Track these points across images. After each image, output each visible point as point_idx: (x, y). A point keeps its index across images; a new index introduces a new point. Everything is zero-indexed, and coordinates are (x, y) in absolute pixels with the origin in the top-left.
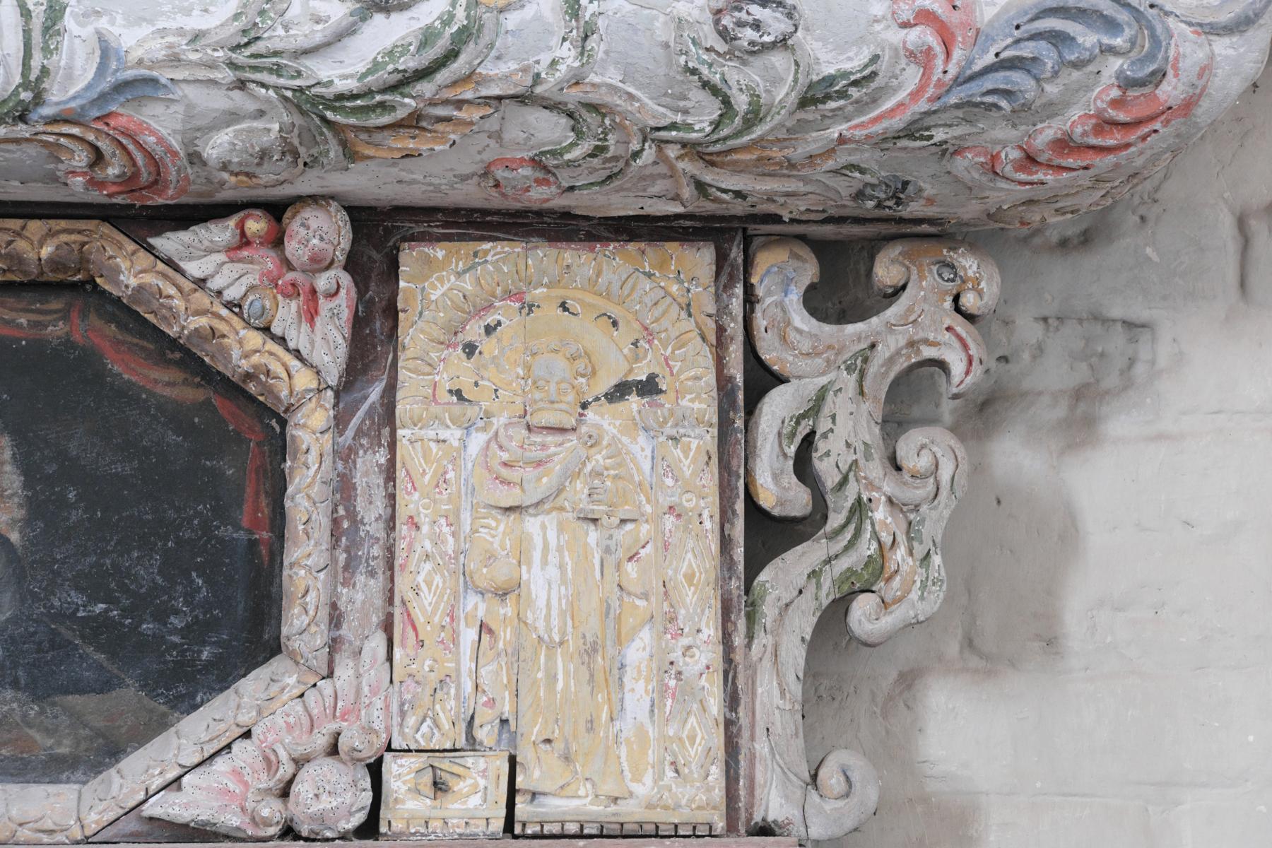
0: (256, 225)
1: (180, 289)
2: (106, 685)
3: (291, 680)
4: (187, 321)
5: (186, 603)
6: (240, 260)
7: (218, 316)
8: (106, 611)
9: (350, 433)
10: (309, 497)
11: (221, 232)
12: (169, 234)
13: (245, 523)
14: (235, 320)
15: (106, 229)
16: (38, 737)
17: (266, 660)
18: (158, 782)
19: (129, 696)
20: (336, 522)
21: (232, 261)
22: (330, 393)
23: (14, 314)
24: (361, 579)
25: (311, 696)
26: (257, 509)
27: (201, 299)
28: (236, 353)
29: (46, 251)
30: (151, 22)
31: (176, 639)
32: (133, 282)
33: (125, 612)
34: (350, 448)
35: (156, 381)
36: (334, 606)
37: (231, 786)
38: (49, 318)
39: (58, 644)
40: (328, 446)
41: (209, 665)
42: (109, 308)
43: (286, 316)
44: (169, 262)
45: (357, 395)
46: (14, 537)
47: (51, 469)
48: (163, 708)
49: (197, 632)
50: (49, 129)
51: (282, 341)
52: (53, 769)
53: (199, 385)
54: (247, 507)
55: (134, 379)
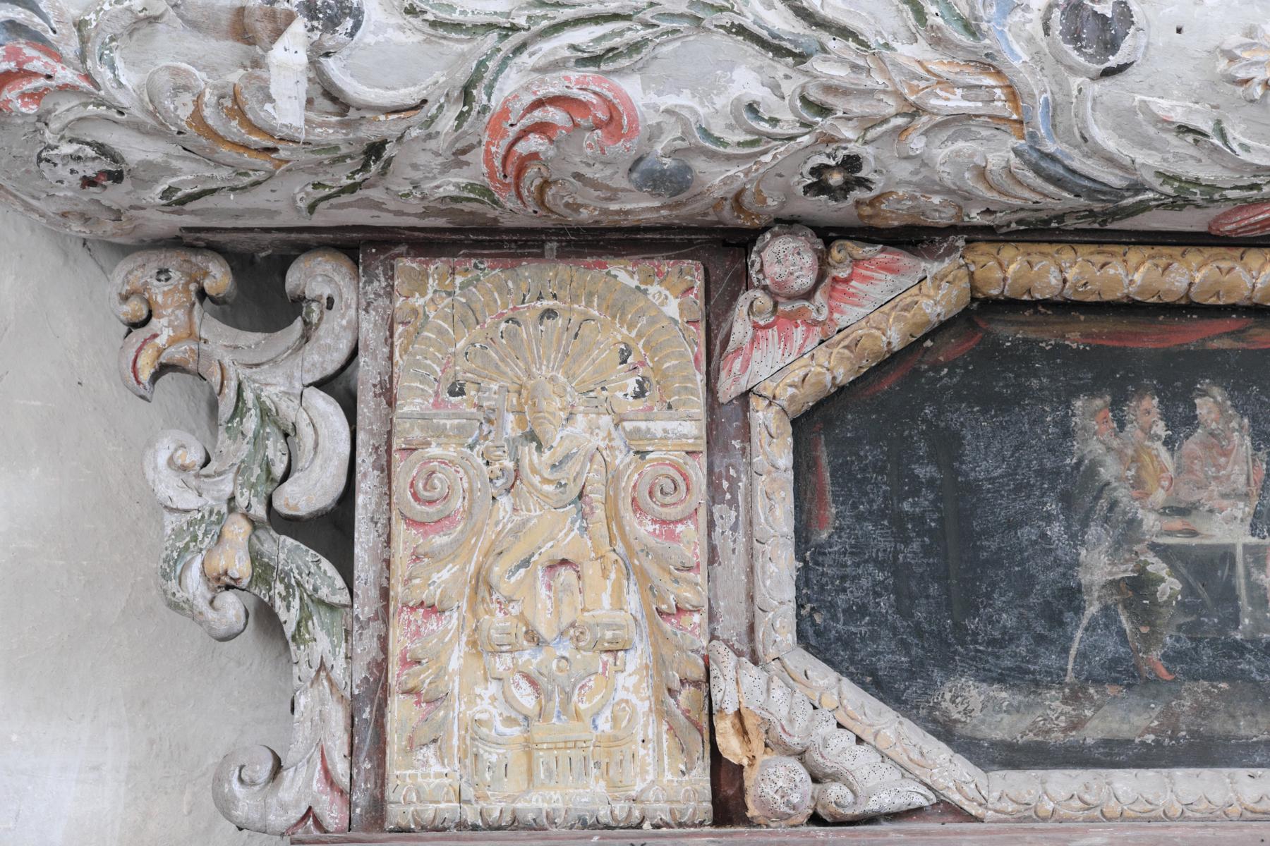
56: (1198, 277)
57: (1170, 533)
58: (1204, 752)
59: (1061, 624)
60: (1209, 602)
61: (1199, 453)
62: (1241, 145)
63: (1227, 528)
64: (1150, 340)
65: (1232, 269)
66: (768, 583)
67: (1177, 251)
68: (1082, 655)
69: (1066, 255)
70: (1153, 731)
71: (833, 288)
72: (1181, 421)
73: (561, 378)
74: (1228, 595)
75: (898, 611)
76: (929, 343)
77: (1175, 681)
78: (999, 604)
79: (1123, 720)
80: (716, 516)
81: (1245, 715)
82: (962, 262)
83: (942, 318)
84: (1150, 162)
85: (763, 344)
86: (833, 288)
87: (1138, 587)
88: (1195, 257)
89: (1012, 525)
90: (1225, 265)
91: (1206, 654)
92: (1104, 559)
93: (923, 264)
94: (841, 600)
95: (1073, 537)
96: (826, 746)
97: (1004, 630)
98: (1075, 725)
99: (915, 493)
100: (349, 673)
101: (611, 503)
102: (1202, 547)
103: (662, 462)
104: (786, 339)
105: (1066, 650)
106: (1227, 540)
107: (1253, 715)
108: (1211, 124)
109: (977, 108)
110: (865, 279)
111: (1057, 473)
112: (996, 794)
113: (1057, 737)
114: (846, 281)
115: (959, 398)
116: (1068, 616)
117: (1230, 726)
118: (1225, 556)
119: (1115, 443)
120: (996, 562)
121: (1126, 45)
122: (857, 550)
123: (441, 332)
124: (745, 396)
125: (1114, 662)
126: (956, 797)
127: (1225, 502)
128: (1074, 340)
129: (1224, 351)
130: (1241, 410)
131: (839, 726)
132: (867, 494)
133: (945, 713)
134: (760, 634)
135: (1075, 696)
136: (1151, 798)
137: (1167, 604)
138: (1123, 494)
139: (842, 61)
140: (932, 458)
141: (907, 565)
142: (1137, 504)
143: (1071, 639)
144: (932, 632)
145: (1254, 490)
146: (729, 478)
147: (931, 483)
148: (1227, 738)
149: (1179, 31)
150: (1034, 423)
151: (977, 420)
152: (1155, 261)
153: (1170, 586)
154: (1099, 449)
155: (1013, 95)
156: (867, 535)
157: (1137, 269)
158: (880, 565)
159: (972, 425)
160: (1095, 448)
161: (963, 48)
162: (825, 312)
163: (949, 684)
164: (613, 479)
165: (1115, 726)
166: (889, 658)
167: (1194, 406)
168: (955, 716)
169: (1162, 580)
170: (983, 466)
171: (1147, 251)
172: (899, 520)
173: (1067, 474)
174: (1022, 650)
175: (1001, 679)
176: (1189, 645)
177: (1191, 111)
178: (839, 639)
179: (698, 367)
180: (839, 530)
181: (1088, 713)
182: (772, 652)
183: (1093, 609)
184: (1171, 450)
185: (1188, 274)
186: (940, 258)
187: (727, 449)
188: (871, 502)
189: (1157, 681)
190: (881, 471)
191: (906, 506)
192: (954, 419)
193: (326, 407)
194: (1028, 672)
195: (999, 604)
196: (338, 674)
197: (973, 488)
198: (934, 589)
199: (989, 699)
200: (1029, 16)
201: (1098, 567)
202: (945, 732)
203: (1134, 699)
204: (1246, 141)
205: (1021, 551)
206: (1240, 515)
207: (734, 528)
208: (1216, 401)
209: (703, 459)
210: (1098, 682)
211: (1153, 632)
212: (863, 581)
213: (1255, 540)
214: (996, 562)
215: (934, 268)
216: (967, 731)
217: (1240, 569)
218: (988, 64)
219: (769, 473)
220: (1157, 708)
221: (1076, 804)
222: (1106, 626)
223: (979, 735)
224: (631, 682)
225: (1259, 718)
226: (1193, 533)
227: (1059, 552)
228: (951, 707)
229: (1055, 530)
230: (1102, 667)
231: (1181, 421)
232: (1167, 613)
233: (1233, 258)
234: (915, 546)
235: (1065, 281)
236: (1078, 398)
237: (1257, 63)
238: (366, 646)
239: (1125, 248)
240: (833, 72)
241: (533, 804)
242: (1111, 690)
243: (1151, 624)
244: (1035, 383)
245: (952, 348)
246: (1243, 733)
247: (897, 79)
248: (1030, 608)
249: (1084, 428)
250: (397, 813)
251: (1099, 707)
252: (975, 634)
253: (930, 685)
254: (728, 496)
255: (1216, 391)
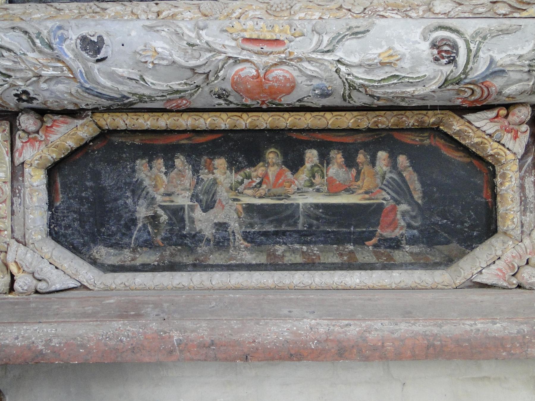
0: (503, 112)
1: (472, 130)
2: (448, 243)
3: (511, 243)
4: (472, 139)
5: (469, 219)
6: (495, 122)
7: (485, 138)
8: (447, 222)
9: (523, 172)
10: (513, 191)
11: (492, 114)
12: (470, 114)
13: (484, 196)
14: (490, 139)
15: (451, 113)
16: (430, 257)
17: (492, 236)
18: (475, 272)
19: (454, 246)
20: (521, 198)
21: (491, 122)
22: (518, 160)
23: (415, 138)
24: (528, 214)
25: (518, 248)
26: (487, 193)
27: (479, 133)
28: (489, 150)
29: (432, 120)
30: (505, 52)
31: (466, 229)
32: (458, 128)
33: (452, 222)
34: (523, 176)
35: (456, 156)
36: (521, 222)
37: (500, 274)
38: (425, 138)
39: (436, 232)
40: (518, 176)
41: (476, 237)
42: (442, 135)
43: (507, 139)
44: (469, 122)
45: (524, 161)
46: (420, 202)
47: (429, 182)
48: (464, 249)
49: (472, 228)
50: (465, 86)
51: (504, 145)
52: (435, 266)
53: (468, 157)
54: (485, 192)
55: (450, 156)
56: (168, 122)
57: (165, 201)
58: (173, 267)
59: (130, 229)
60: (176, 222)
61: (175, 177)
62: (152, 83)
63: (183, 200)
64: (161, 141)
65: (178, 120)
66: (30, 221)
67: (160, 114)
68: (136, 239)
69: (124, 116)
70: (157, 261)
71: (47, 130)
72: (170, 166)
74: (182, 220)
75: (80, 226)
76: (91, 144)
77: (164, 246)
78: (111, 224)
79: (148, 258)
80: (14, 201)
81: (185, 256)
82: (91, 119)
83: (94, 136)
84: (125, 89)
85: (25, 148)
86: (47, 130)
87: (155, 218)
88: (166, 116)
89: (116, 200)
90: (176, 118)
91: (174, 238)
92: (144, 210)
93: (76, 121)
94: (63, 223)
95: (135, 203)
96: (42, 270)
97: (113, 232)
98: (133, 260)
99: (86, 190)
102: (174, 206)
104: (33, 146)
105: (131, 237)
106: (182, 203)
107: (188, 256)
108: (138, 77)
109: (59, 74)
110: (57, 126)
111: (130, 184)
112: (100, 282)
113: (128, 263)
114: (51, 127)
115: (101, 161)
116: (132, 227)
117: (181, 259)
118: (182, 208)
119: (149, 174)
120: (111, 211)
121: (103, 51)
122: (68, 208)
124: (23, 163)
125: (146, 241)
126: (86, 284)
127: (183, 192)
128: (137, 141)
129: (185, 144)
130: (189, 163)
131: (50, 263)
132: (71, 191)
133: (94, 256)
134: (27, 237)
135: (134, 251)
136: (145, 283)
137: (163, 223)
138: (150, 190)
139: (9, 60)
140: (91, 180)
141: (84, 213)
142: (155, 193)
143: (133, 234)
144: (90, 233)
145: (192, 188)
146: (18, 189)
147: (91, 188)
148: (180, 263)
149: (123, 45)
150: (123, 168)
151: (106, 167)
152: (154, 118)
153: (164, 217)
154: (144, 176)
155: (70, 70)
156: (71, 203)
157: (148, 120)
158: (75, 212)
159: (105, 170)
160: (143, 175)
161: (49, 54)
162: (44, 137)
163: (95, 248)
165: (146, 260)
166: (77, 241)
167: (174, 162)
168: (97, 257)
169: (162, 216)
170: (108, 182)
171: (151, 114)
172: (81, 199)
173: (134, 184)
174: (118, 238)
175: (111, 246)
176: (169, 235)
177: (130, 73)
178: (62, 235)
179: (7, 155)
180: (63, 202)
181: (137, 256)
182: (31, 241)
183: (140, 225)
184: (166, 176)
185: (163, 122)
186: (83, 119)
187: (18, 180)
188: (73, 193)
189: (159, 246)
190: (76, 184)
191: (83, 195)
192: (99, 167)
194: (120, 244)
195: (111, 224)
197: (103, 189)
198: (91, 220)
199: (107, 252)
200: (72, 42)
201: (142, 212)
202: (94, 262)
203: (152, 251)
204: (153, 81)
205: (119, 208)
206: (187, 195)
207: (20, 204)
208: (181, 160)
209: (9, 184)
210: (141, 247)
211: (158, 231)
212: (70, 218)
213: (191, 203)
214: (111, 211)
215: (80, 122)
216: (101, 262)
217: (186, 212)
218: (58, 59)
219: (30, 187)
220: (158, 254)
221: (123, 285)
222: (144, 230)
223: (104, 263)
225: (190, 257)
226: (172, 201)
227: (130, 208)
228: (96, 254)
229: (129, 201)
230: (142, 242)
231: (170, 166)
232: (163, 226)
233: (178, 116)
234: (86, 207)
235: (126, 124)
236: (137, 159)
237: (148, 56)
239: (143, 113)
240: (7, 64)
242: (144, 249)
243: (158, 230)
244: (124, 156)
245: (99, 144)
246: (185, 261)
247: (29, 65)
248: (121, 225)
249: (140, 170)
251: (141, 254)
252: (104, 233)
253: (90, 249)
254: (18, 195)
255: (181, 157)
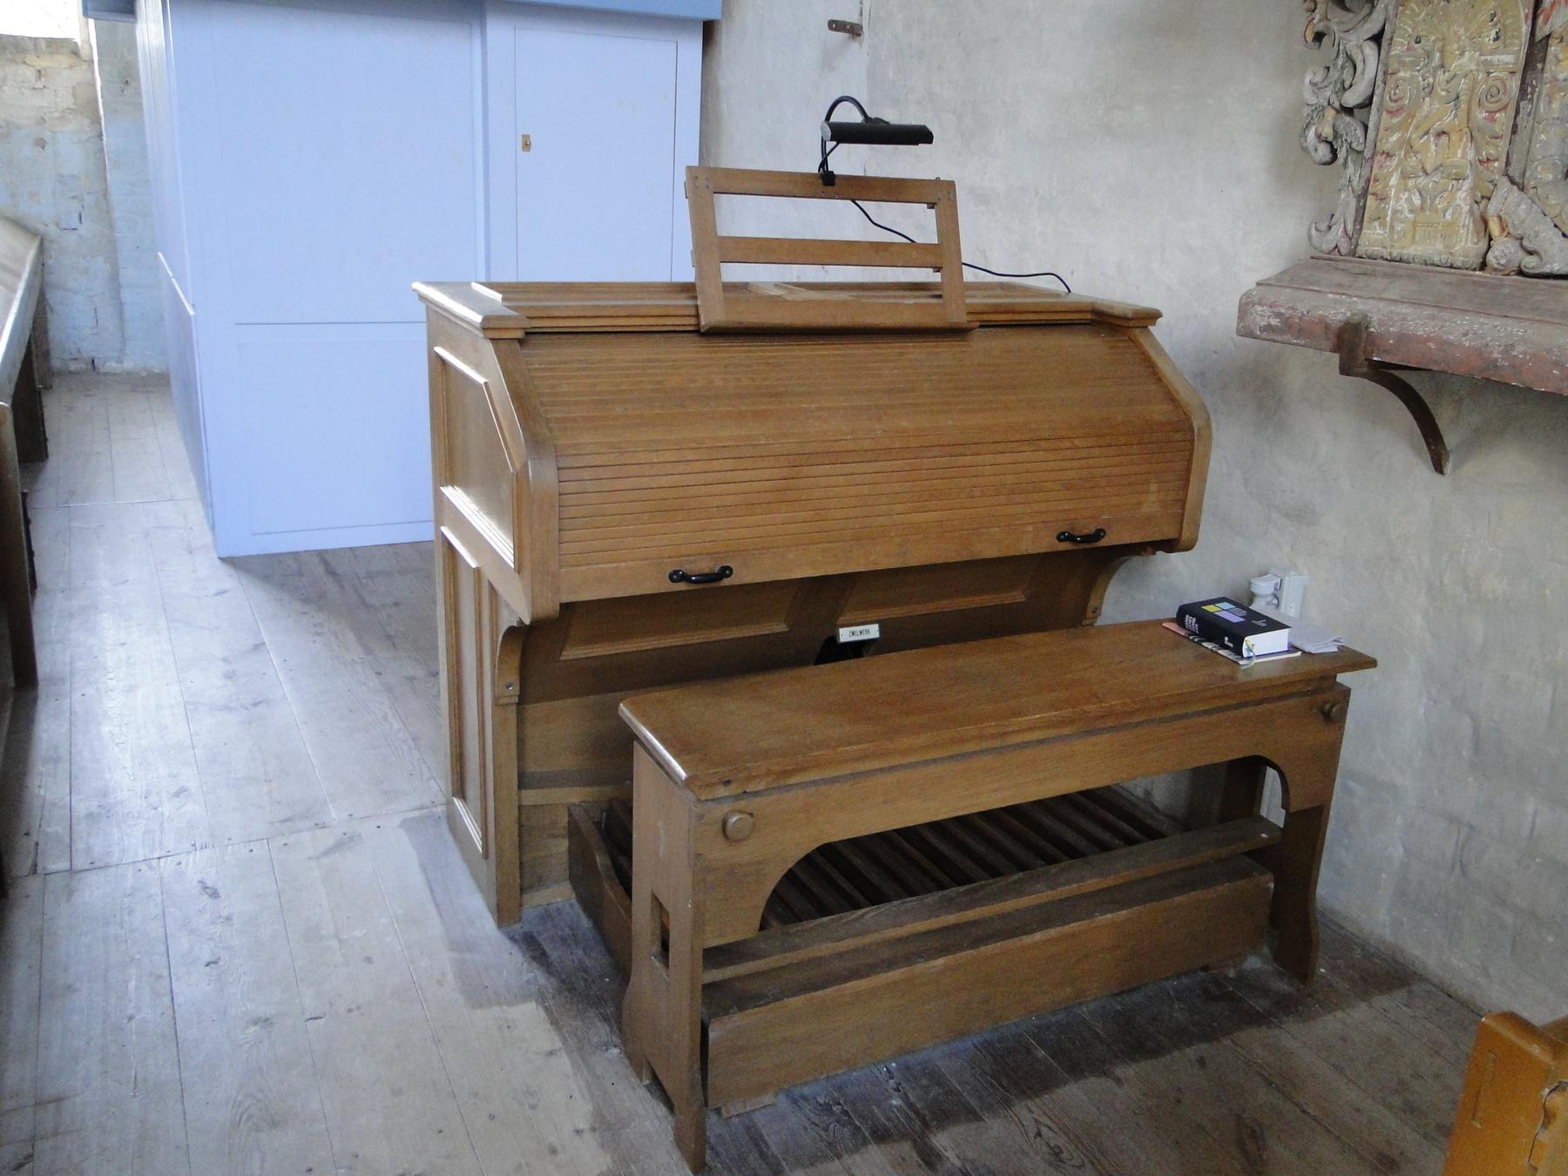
73: (1462, 31)
100: (1358, 184)
101: (1469, 102)
103: (1497, 78)
123: (1413, 10)
164: (1472, 90)
193: (1370, 49)
196: (1355, 183)
209: (1519, 76)
224: (1462, 196)
238: (1366, 171)
241: (1411, 251)
250: (1361, 250)
